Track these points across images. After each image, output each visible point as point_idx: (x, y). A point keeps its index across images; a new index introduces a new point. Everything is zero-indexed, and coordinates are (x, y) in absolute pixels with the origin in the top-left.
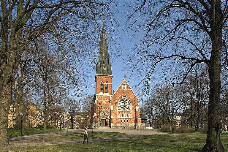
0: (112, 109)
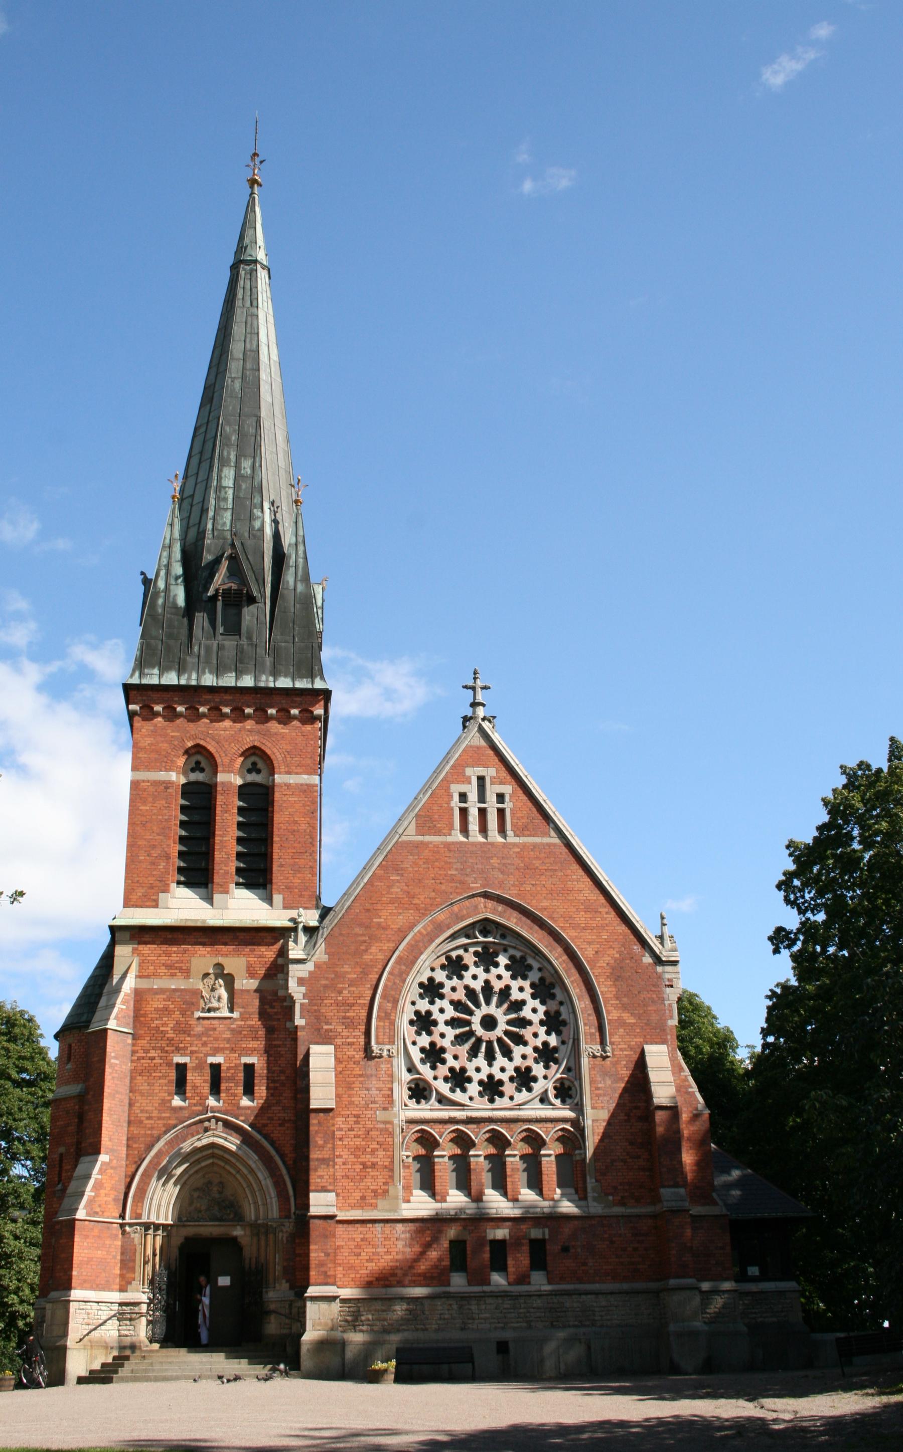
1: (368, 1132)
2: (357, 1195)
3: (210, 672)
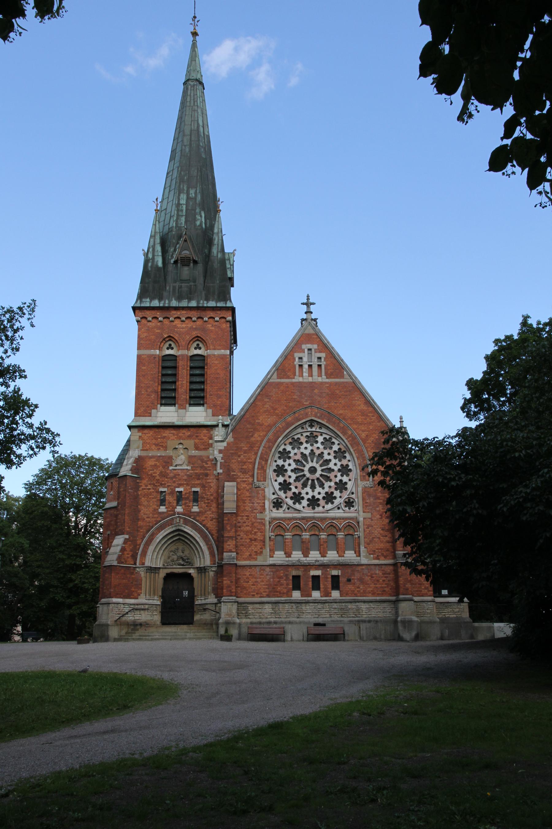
0: (230, 506)
1: (253, 524)
2: (248, 554)
3: (175, 300)
